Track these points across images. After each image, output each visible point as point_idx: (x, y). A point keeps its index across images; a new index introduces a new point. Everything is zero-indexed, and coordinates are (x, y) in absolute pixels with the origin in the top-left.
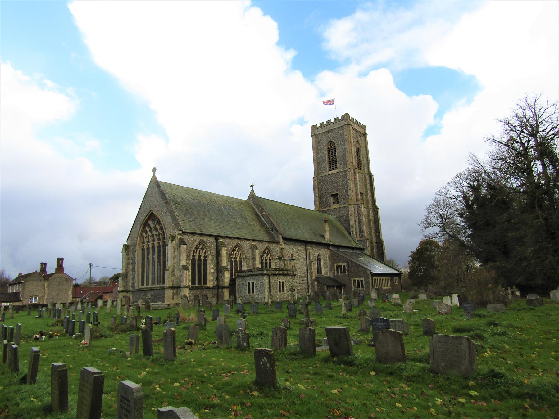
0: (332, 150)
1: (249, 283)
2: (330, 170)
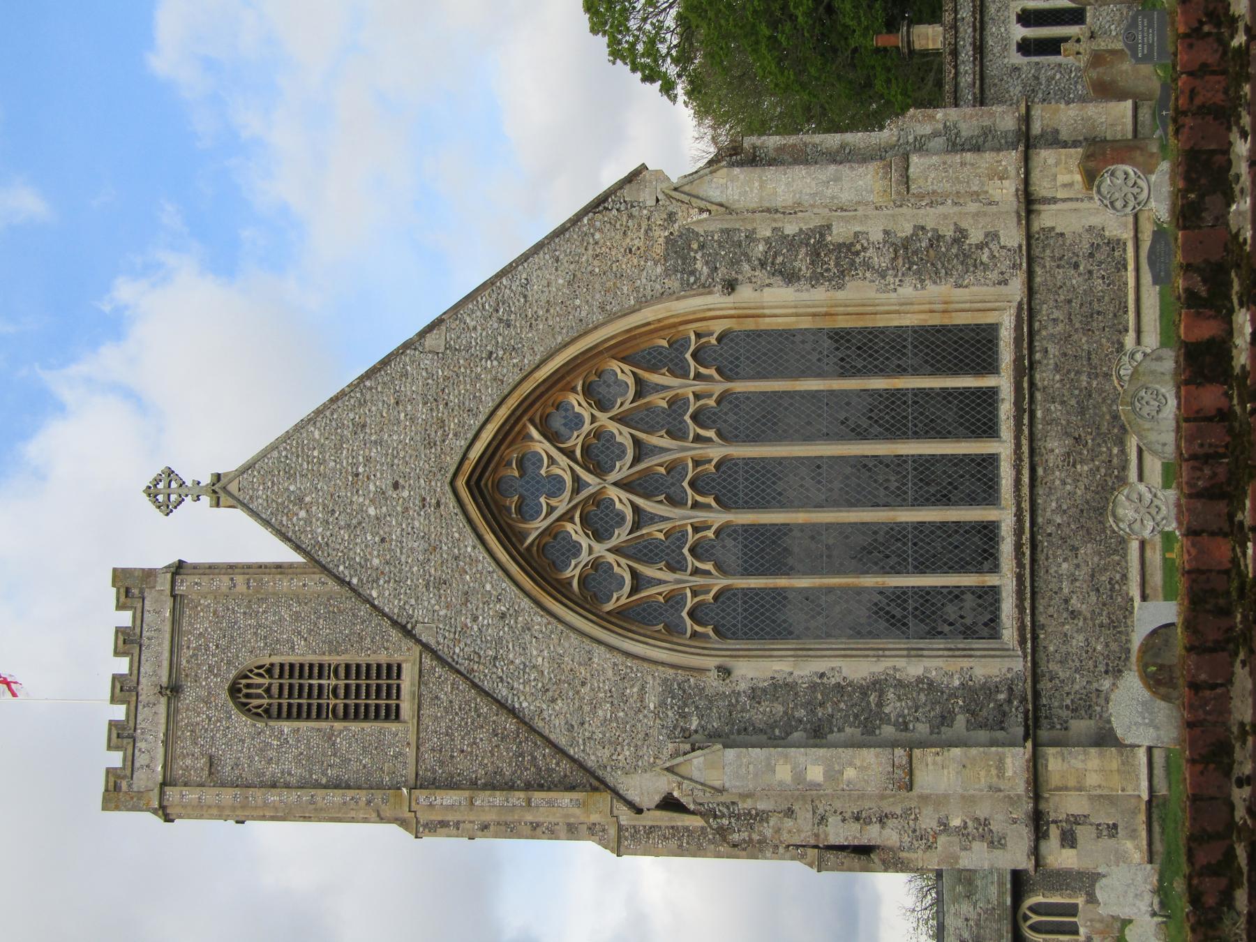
0: (284, 693)
1: (1026, 47)
2: (393, 714)
